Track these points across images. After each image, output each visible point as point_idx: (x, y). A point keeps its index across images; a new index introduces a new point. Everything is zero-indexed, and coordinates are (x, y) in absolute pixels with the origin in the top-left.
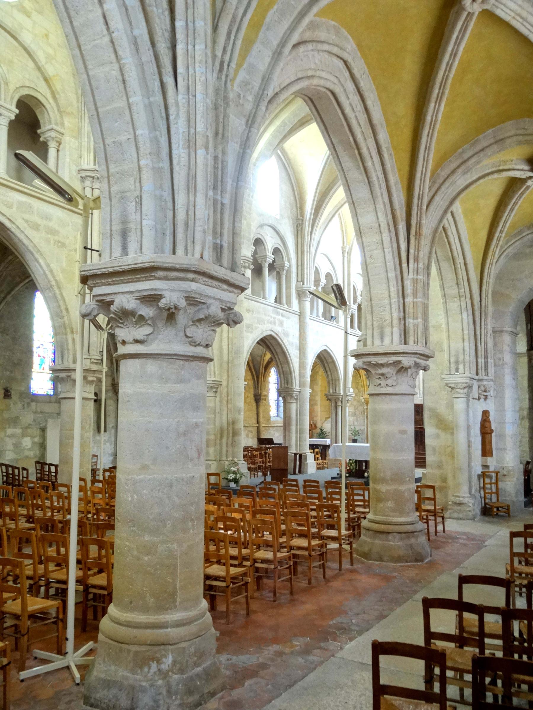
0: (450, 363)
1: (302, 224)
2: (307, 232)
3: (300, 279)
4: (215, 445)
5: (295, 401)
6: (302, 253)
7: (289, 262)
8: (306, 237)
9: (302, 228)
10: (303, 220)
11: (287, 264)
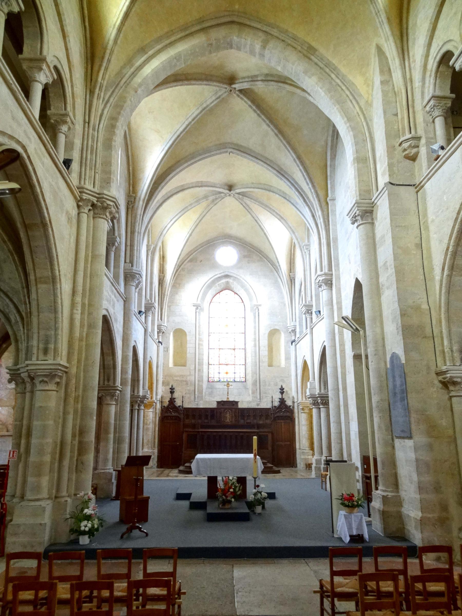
0: (452, 351)
1: (134, 202)
2: (140, 211)
3: (128, 261)
4: (51, 470)
5: (114, 403)
6: (133, 232)
7: (120, 238)
8: (138, 216)
9: (133, 207)
10: (135, 198)
11: (118, 239)
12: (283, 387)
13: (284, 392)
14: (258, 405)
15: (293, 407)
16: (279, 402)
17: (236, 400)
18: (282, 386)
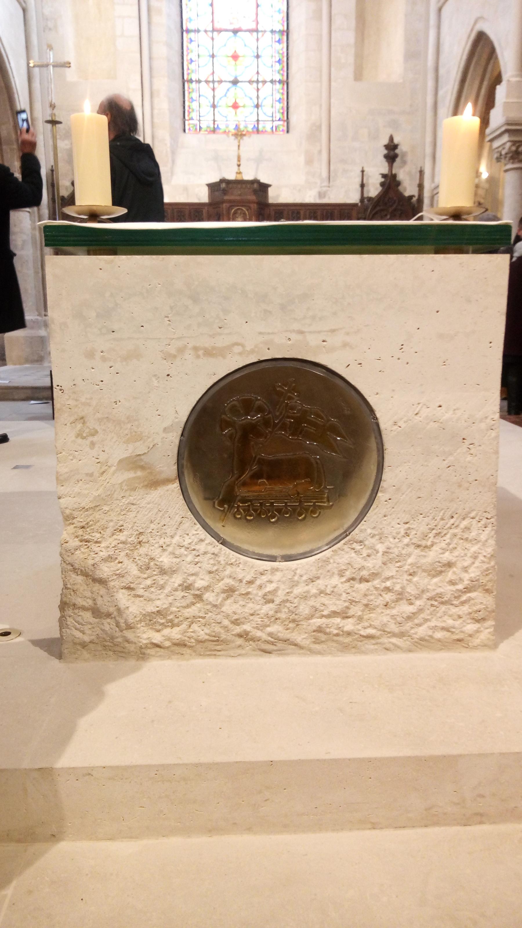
12: (396, 141)
13: (396, 156)
14: (321, 195)
15: (420, 200)
16: (382, 184)
17: (263, 180)
18: (391, 139)
